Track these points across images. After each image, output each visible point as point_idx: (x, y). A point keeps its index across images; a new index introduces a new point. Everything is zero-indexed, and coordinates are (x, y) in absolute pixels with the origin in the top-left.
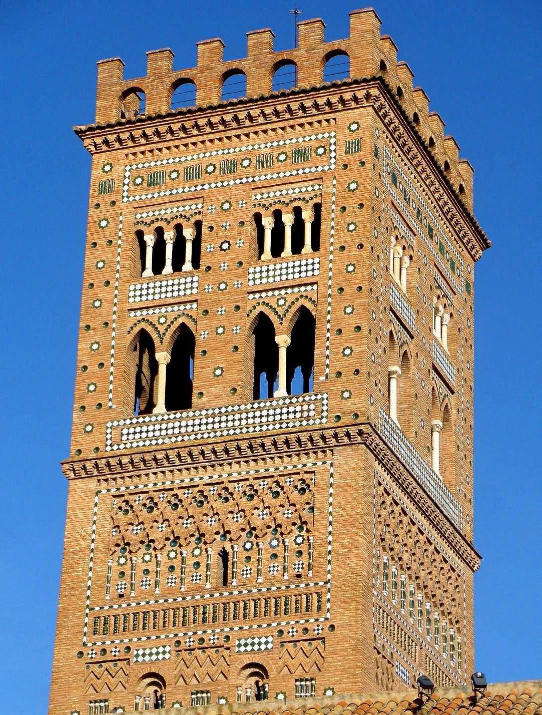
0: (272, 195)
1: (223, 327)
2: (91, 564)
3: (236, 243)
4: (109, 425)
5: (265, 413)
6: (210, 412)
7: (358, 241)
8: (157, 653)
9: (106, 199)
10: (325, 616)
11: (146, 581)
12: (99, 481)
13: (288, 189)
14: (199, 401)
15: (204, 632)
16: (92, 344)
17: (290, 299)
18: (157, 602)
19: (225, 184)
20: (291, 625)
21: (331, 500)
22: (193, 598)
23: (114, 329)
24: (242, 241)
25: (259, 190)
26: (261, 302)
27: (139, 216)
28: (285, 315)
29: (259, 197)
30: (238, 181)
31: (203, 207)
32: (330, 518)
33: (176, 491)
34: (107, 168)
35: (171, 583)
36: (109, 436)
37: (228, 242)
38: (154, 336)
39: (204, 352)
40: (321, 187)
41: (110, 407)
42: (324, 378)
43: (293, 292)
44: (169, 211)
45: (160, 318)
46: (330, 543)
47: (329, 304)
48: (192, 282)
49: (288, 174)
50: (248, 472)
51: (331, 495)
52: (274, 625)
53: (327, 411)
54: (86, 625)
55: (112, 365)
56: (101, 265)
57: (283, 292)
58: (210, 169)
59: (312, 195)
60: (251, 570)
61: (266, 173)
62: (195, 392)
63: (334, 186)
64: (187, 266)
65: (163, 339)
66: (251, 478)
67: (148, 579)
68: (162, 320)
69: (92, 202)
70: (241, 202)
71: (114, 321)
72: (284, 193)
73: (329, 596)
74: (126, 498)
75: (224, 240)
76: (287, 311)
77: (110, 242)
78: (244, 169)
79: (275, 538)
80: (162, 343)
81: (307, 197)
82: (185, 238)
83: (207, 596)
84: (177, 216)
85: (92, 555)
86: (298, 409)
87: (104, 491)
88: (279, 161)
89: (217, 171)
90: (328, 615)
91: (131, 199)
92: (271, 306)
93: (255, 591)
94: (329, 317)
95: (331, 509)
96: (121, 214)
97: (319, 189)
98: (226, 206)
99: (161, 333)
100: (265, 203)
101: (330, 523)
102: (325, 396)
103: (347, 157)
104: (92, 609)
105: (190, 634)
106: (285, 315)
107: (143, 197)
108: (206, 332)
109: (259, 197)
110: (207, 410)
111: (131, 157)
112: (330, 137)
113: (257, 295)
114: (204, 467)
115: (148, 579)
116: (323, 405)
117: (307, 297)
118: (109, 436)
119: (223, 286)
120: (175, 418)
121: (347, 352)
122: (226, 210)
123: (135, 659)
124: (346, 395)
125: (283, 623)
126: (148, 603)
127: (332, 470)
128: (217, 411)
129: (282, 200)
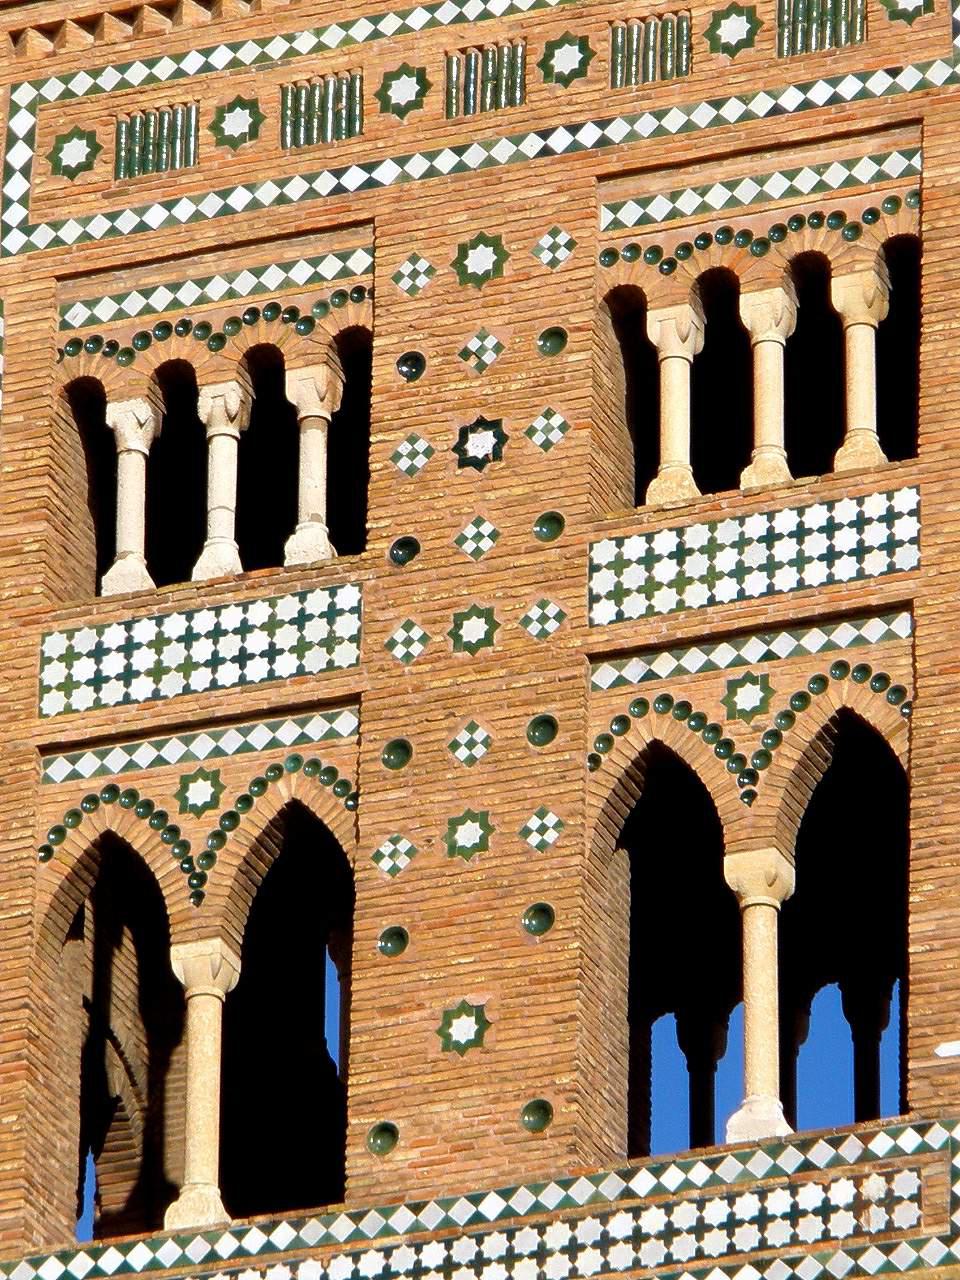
0: (688, 202)
1: (482, 819)
3: (531, 432)
5: (685, 1215)
6: (431, 1216)
14: (380, 1167)
17: (788, 683)
19: (474, 157)
24: (556, 421)
25: (630, 184)
26: (651, 697)
27: (78, 315)
28: (764, 757)
29: (630, 213)
30: (532, 145)
31: (371, 269)
38: (164, 866)
39: (398, 937)
40: (916, 161)
43: (799, 651)
44: (217, 288)
45: (185, 782)
48: (332, 613)
49: (761, 105)
57: (754, 649)
58: (404, 90)
59: (876, 200)
61: (660, 104)
62: (359, 1122)
64: (309, 541)
65: (202, 878)
68: (199, 792)
70: (546, 241)
72: (746, 191)
75: (472, 416)
76: (775, 736)
78: (560, 91)
80: (198, 897)
81: (853, 207)
82: (292, 410)
84: (254, 313)
86: (842, 1193)
88: (717, 46)
89: (435, 101)
91: (42, 236)
92: (701, 719)
97: (909, 171)
98: (480, 260)
99: (195, 852)
100: (658, 240)
106: (764, 757)
107: (99, 227)
108: (404, 845)
109: (630, 213)
110: (417, 1208)
111: (38, 43)
113: (634, 669)
117: (864, 670)
119: (473, 630)
120: (269, 1248)
122: (479, 280)
129: (739, 224)
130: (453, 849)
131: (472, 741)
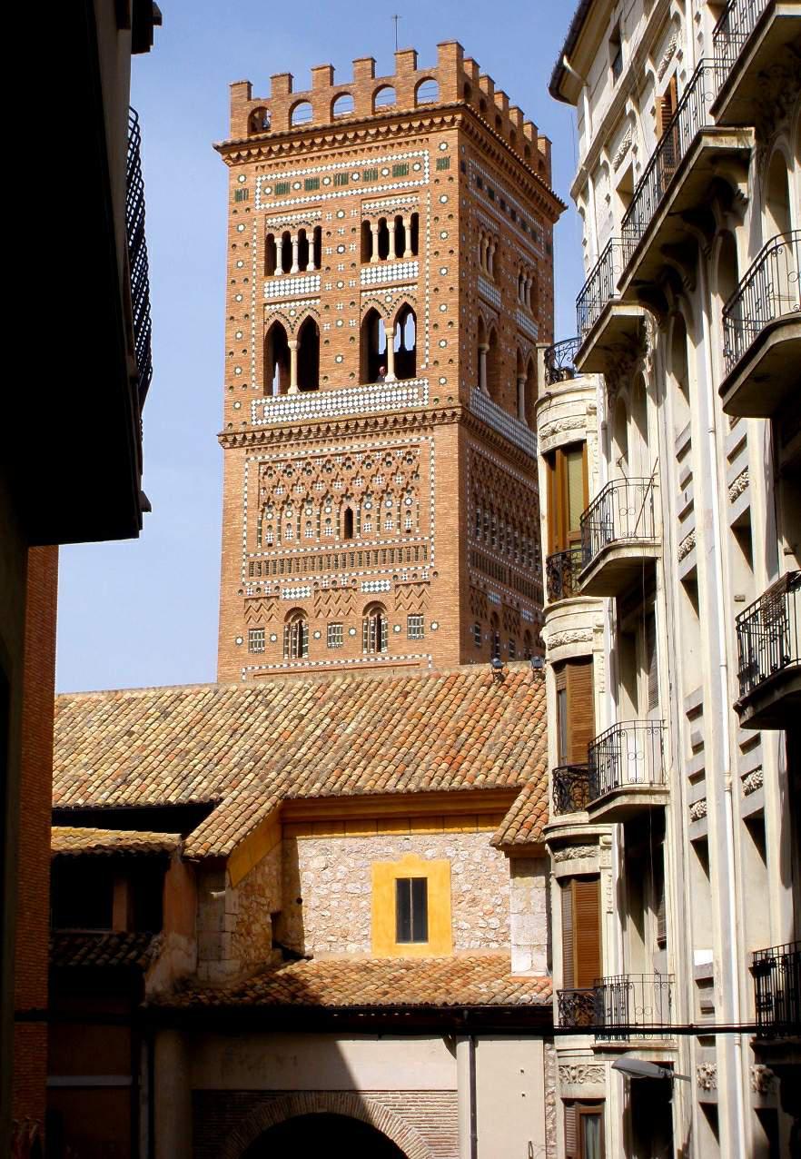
0: (378, 205)
2: (245, 519)
4: (254, 402)
5: (378, 395)
6: (334, 394)
7: (450, 247)
8: (301, 592)
12: (247, 450)
13: (390, 200)
15: (336, 576)
17: (395, 297)
18: (298, 550)
19: (339, 194)
20: (404, 571)
21: (433, 469)
22: (327, 548)
23: (253, 321)
30: (350, 193)
32: (433, 485)
33: (309, 460)
34: (242, 179)
36: (254, 413)
37: (342, 246)
38: (286, 326)
39: (327, 342)
46: (432, 505)
47: (427, 302)
48: (315, 281)
50: (366, 445)
52: (390, 571)
54: (244, 568)
55: (253, 351)
56: (240, 264)
57: (390, 290)
58: (327, 181)
59: (411, 206)
62: (321, 376)
63: (429, 198)
64: (311, 266)
66: (368, 450)
68: (293, 313)
71: (253, 314)
73: (433, 548)
74: (270, 464)
77: (247, 244)
79: (389, 500)
81: (407, 207)
83: (337, 547)
85: (245, 511)
86: (405, 392)
87: (252, 459)
89: (332, 183)
90: (433, 564)
91: (263, 206)
93: (375, 543)
94: (427, 313)
95: (433, 477)
96: (255, 219)
98: (341, 214)
101: (432, 489)
102: (426, 381)
103: (439, 173)
104: (248, 556)
105: (325, 577)
109: (367, 206)
112: (424, 155)
113: (369, 293)
114: (331, 440)
118: (254, 413)
121: (443, 344)
123: (283, 597)
124: (443, 381)
125: (398, 570)
126: (291, 551)
127: (433, 445)
129: (387, 209)
130: (337, 326)
131: (340, 306)
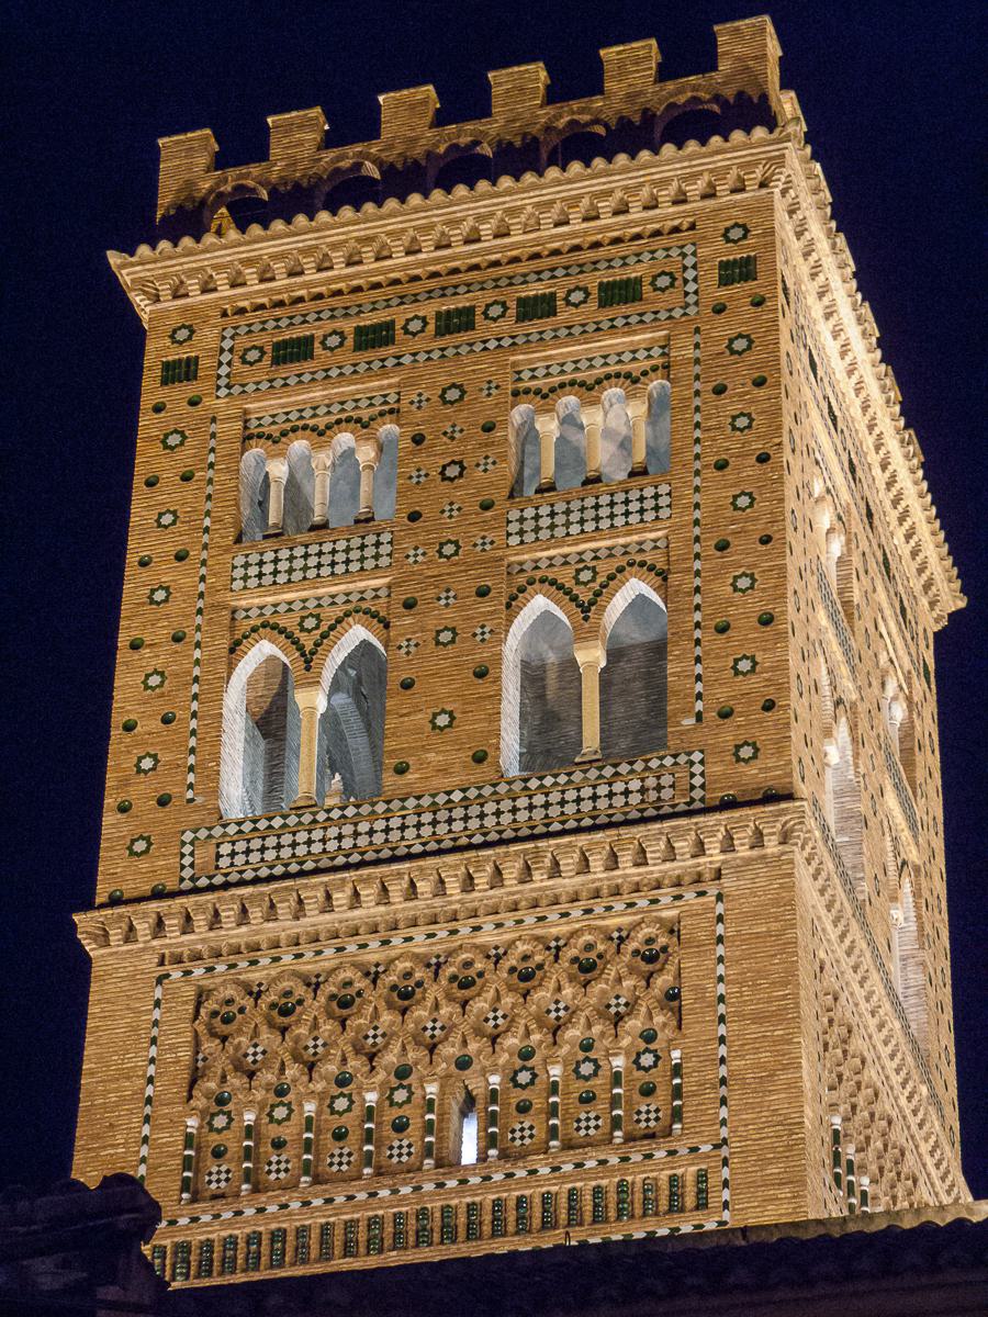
2: (146, 1130)
4: (188, 836)
9: (180, 392)
10: (717, 1219)
11: (278, 1162)
16: (147, 676)
21: (721, 970)
31: (398, 401)
32: (722, 1009)
35: (340, 1164)
36: (187, 861)
40: (666, 350)
41: (191, 801)
42: (692, 721)
45: (303, 619)
51: (721, 960)
53: (703, 786)
60: (531, 1128)
67: (283, 1158)
69: (147, 401)
73: (726, 1173)
85: (148, 1110)
95: (721, 989)
97: (664, 354)
99: (307, 649)
101: (722, 1019)
102: (697, 757)
103: (724, 292)
115: (283, 1158)
116: (693, 775)
118: (187, 861)
121: (744, 666)
124: (746, 752)
127: (720, 909)
128: (442, 799)
